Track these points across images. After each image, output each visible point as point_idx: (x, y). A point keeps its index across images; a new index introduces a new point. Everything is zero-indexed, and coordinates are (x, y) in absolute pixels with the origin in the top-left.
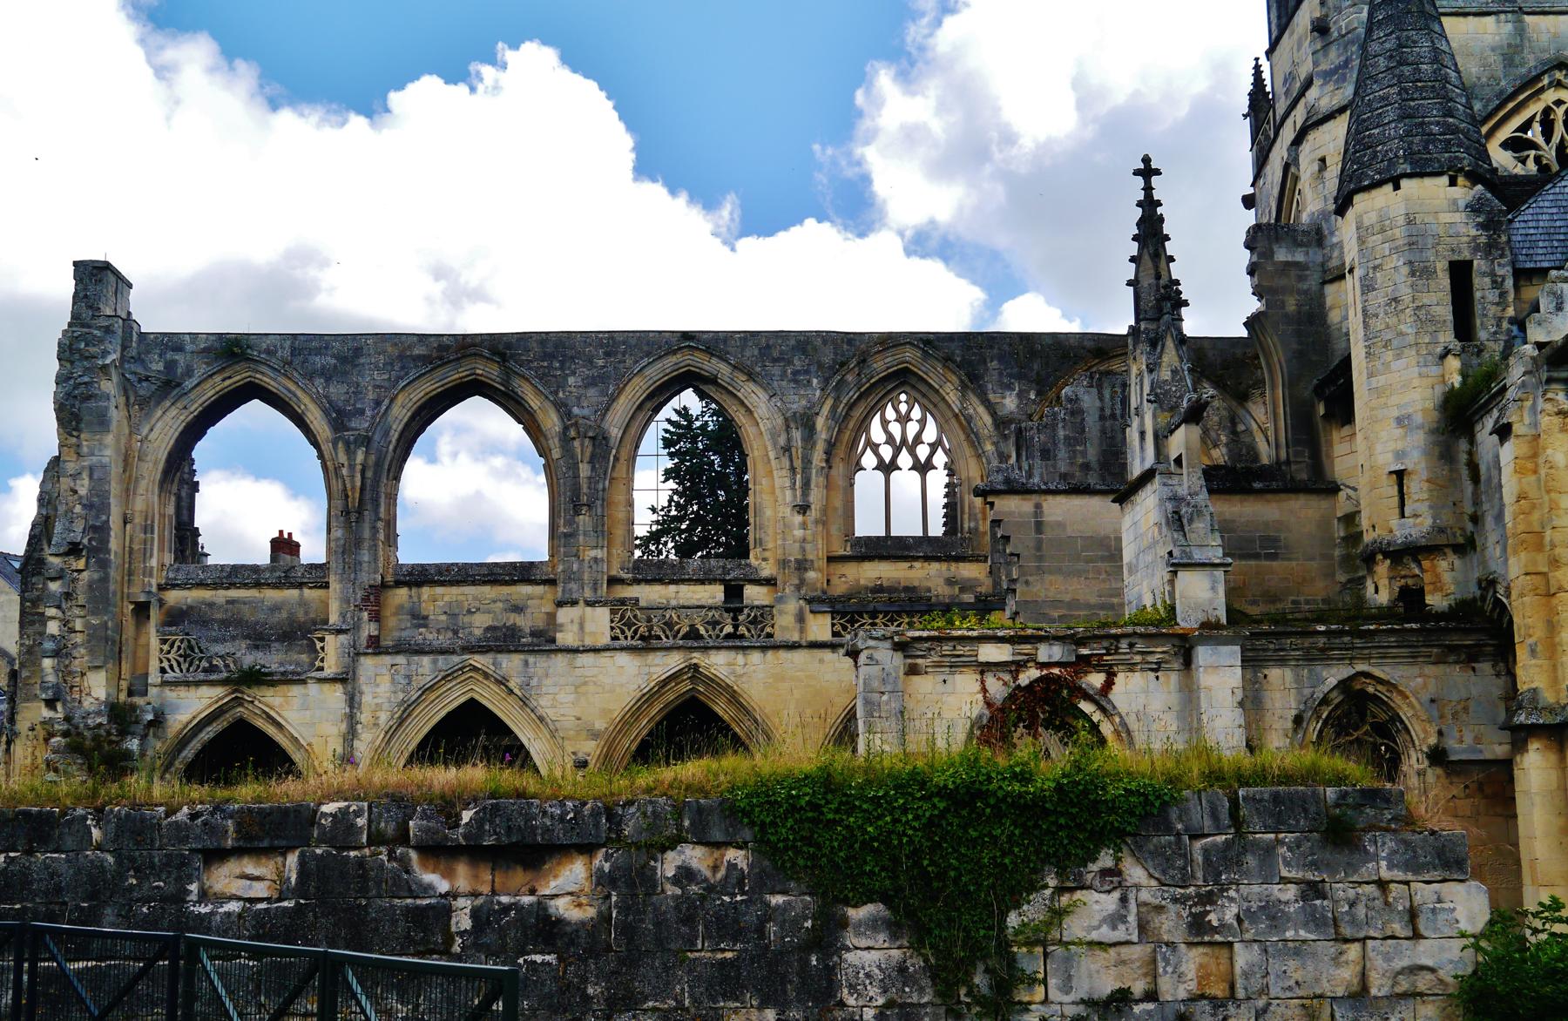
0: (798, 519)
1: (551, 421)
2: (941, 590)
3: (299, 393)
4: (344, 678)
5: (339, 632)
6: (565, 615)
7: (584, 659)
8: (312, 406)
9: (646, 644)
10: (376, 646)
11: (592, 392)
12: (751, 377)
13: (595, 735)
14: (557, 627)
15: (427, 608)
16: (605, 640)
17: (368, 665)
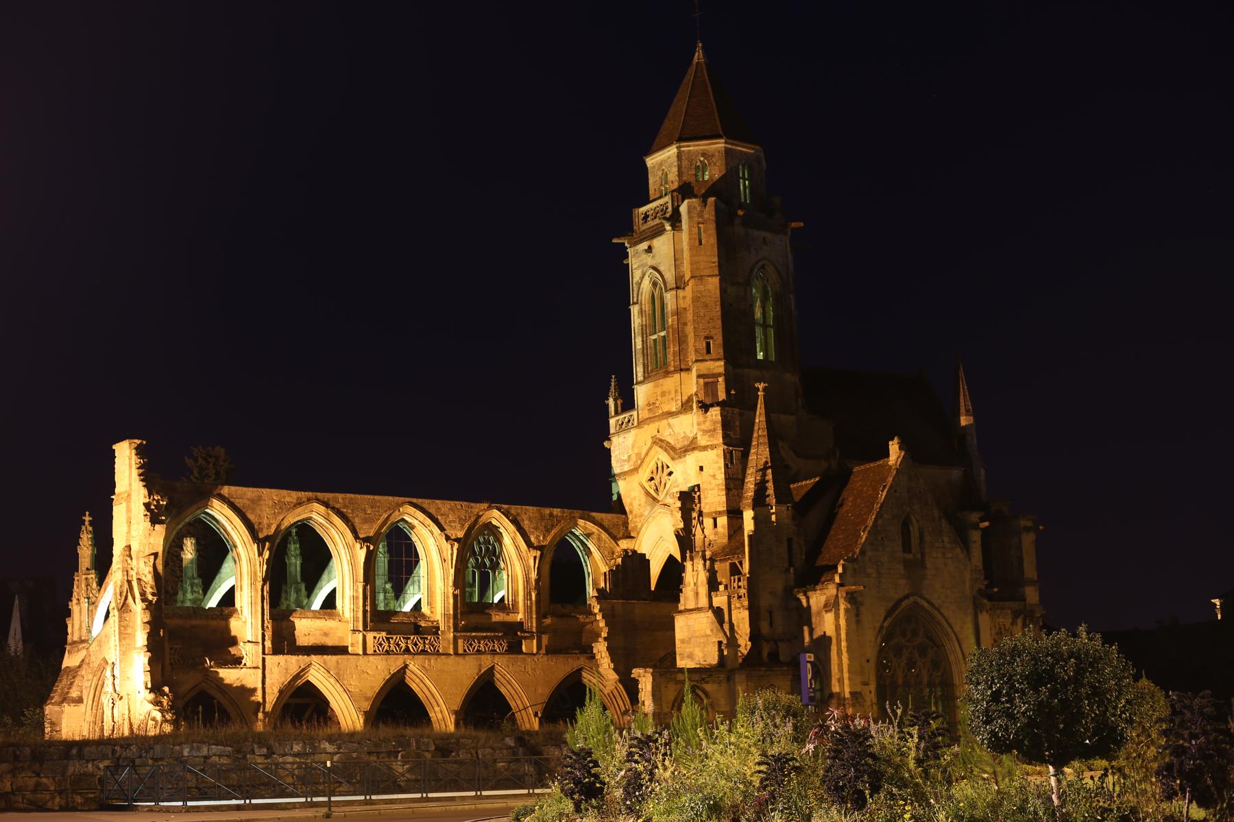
13: (367, 699)
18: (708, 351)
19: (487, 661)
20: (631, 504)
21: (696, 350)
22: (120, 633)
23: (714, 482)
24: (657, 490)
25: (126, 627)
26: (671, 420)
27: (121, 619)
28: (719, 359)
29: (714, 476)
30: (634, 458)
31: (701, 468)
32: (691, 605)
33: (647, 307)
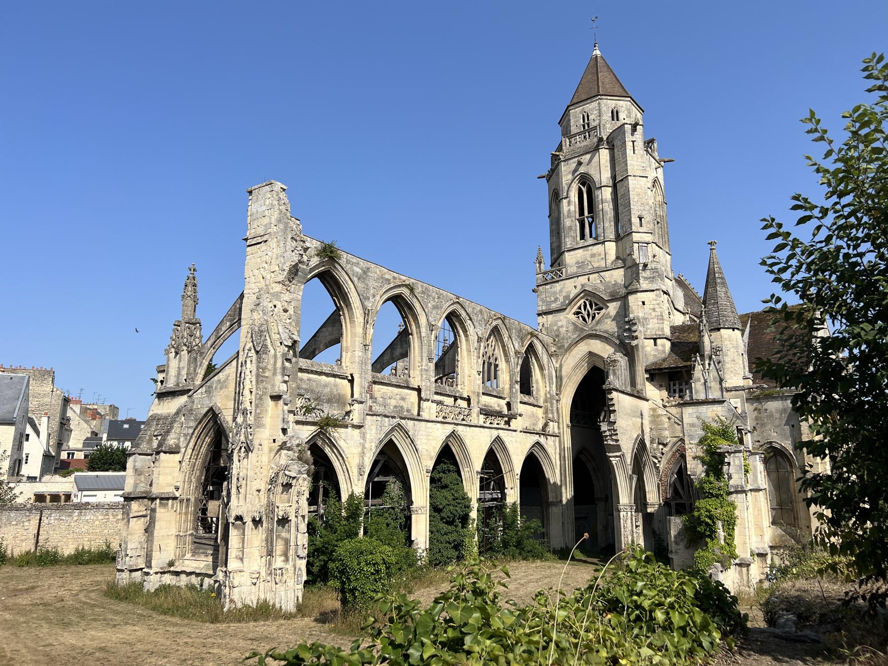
3: (350, 282)
4: (359, 427)
6: (425, 405)
11: (434, 312)
12: (471, 319)
15: (377, 395)
18: (641, 226)
19: (495, 433)
20: (558, 330)
22: (258, 376)
25: (264, 369)
29: (654, 310)
30: (561, 299)
31: (644, 303)
32: (702, 397)
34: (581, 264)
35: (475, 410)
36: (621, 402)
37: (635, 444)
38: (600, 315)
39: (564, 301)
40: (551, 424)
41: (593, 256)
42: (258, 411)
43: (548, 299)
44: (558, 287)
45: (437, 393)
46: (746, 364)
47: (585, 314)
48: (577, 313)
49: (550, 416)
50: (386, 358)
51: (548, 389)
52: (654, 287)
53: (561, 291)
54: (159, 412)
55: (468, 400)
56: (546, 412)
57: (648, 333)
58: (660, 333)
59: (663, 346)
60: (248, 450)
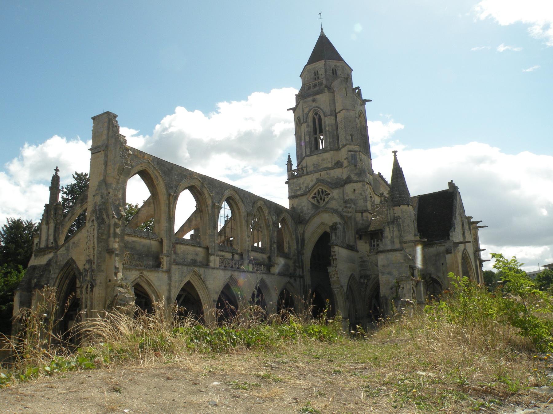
0: (248, 239)
1: (209, 202)
2: (261, 260)
3: (159, 177)
5: (168, 256)
7: (215, 271)
8: (161, 182)
9: (225, 268)
10: (176, 263)
13: (217, 293)
14: (208, 261)
16: (218, 266)
17: (174, 267)
20: (302, 209)
21: (347, 140)
22: (98, 238)
23: (361, 197)
24: (318, 202)
25: (102, 234)
26: (328, 171)
27: (99, 228)
28: (356, 145)
29: (361, 194)
30: (304, 188)
31: (355, 190)
32: (389, 247)
33: (311, 124)
34: (316, 166)
35: (246, 261)
36: (340, 253)
37: (349, 280)
38: (328, 199)
39: (306, 190)
40: (298, 270)
41: (323, 160)
42: (99, 261)
43: (296, 188)
44: (301, 180)
45: (220, 250)
46: (416, 227)
47: (319, 199)
48: (314, 197)
49: (297, 264)
50: (185, 228)
51: (296, 247)
52: (361, 179)
53: (303, 183)
54: (35, 264)
55: (241, 255)
56: (294, 263)
57: (358, 209)
58: (365, 209)
59: (367, 217)
60: (92, 287)
